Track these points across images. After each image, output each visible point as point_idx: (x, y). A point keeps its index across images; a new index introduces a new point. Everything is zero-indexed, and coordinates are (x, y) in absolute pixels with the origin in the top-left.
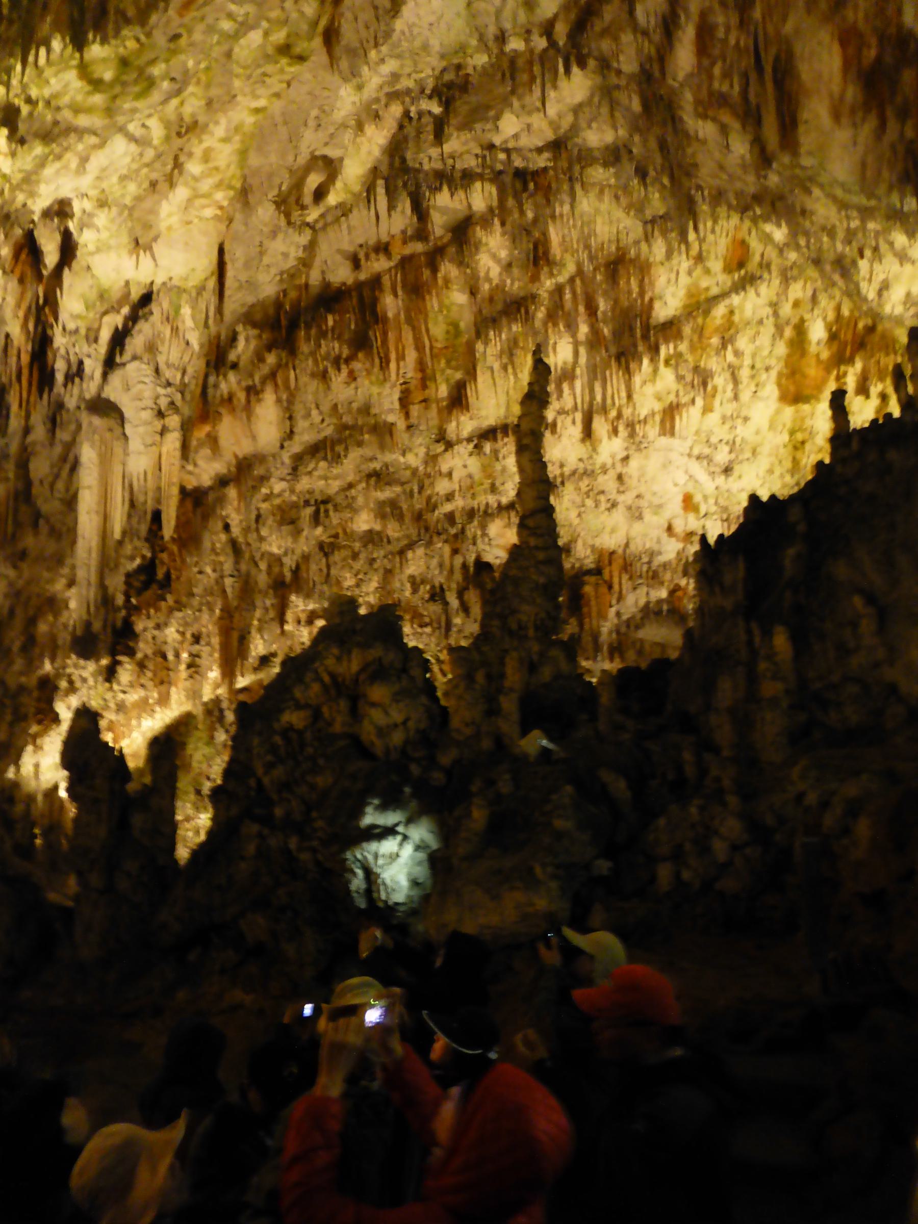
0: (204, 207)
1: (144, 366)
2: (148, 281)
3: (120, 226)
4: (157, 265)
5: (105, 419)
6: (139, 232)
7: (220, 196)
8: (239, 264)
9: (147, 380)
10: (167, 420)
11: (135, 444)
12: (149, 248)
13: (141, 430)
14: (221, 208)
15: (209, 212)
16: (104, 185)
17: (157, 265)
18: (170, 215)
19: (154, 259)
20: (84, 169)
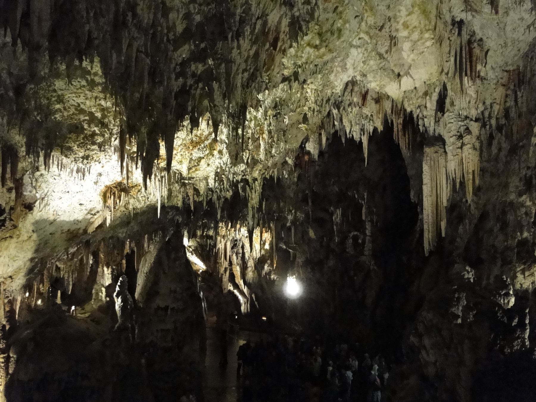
0: (423, 43)
1: (451, 114)
2: (413, 88)
3: (381, 76)
4: (414, 80)
5: (432, 148)
6: (396, 71)
7: (427, 35)
8: (494, 36)
9: (452, 121)
10: (464, 139)
11: (450, 156)
12: (407, 74)
13: (451, 148)
14: (433, 39)
15: (429, 43)
16: (359, 68)
17: (414, 80)
18: (408, 56)
19: (412, 78)
20: (346, 68)
